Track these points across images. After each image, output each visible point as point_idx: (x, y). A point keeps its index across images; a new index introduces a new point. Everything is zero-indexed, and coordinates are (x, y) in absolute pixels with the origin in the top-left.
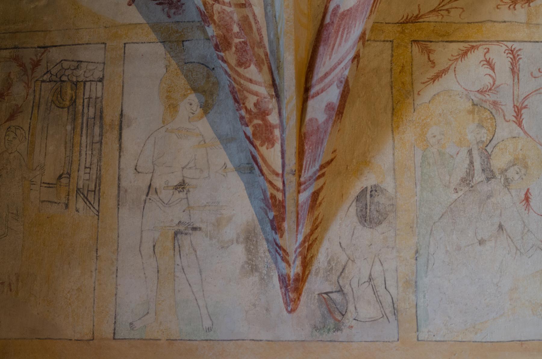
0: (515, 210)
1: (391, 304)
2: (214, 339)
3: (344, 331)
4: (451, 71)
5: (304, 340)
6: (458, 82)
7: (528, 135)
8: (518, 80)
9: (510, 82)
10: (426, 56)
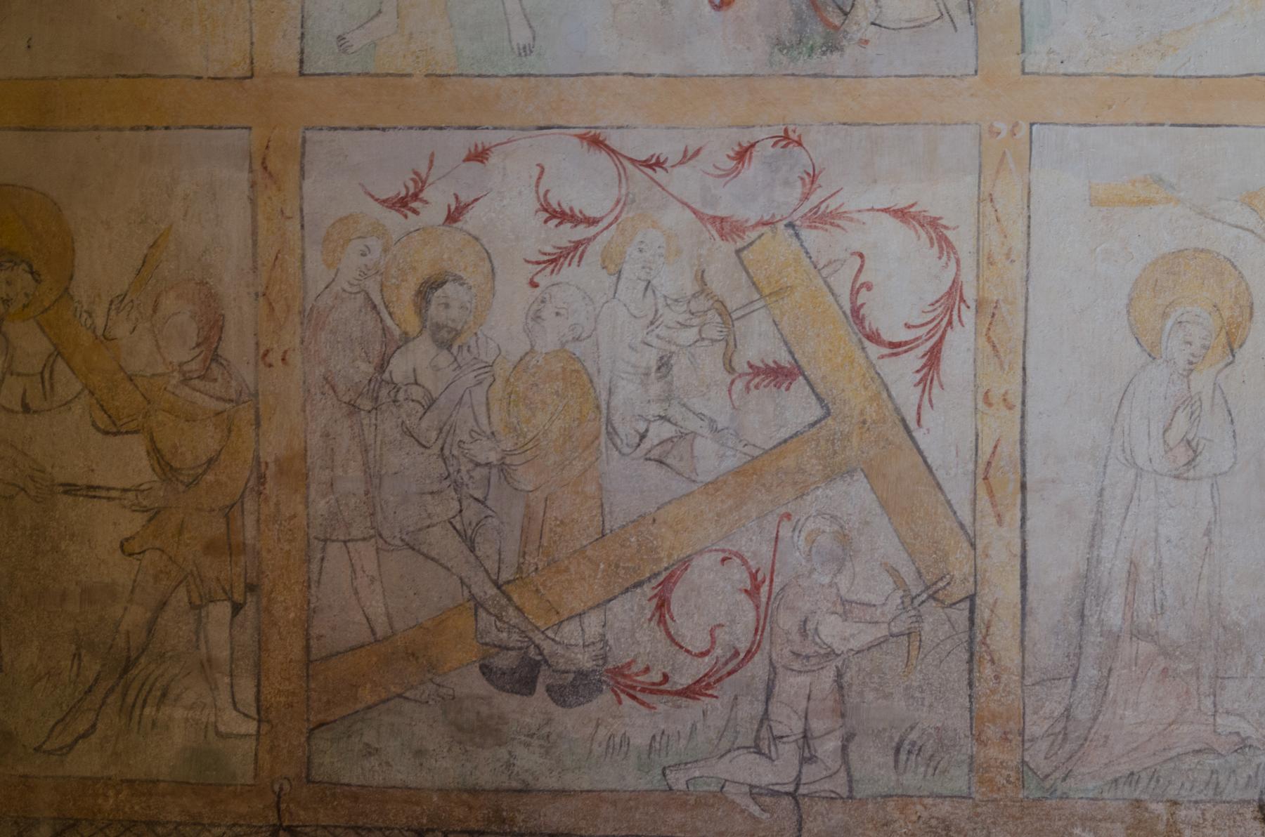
2: (537, 73)
3: (848, 51)
5: (751, 73)
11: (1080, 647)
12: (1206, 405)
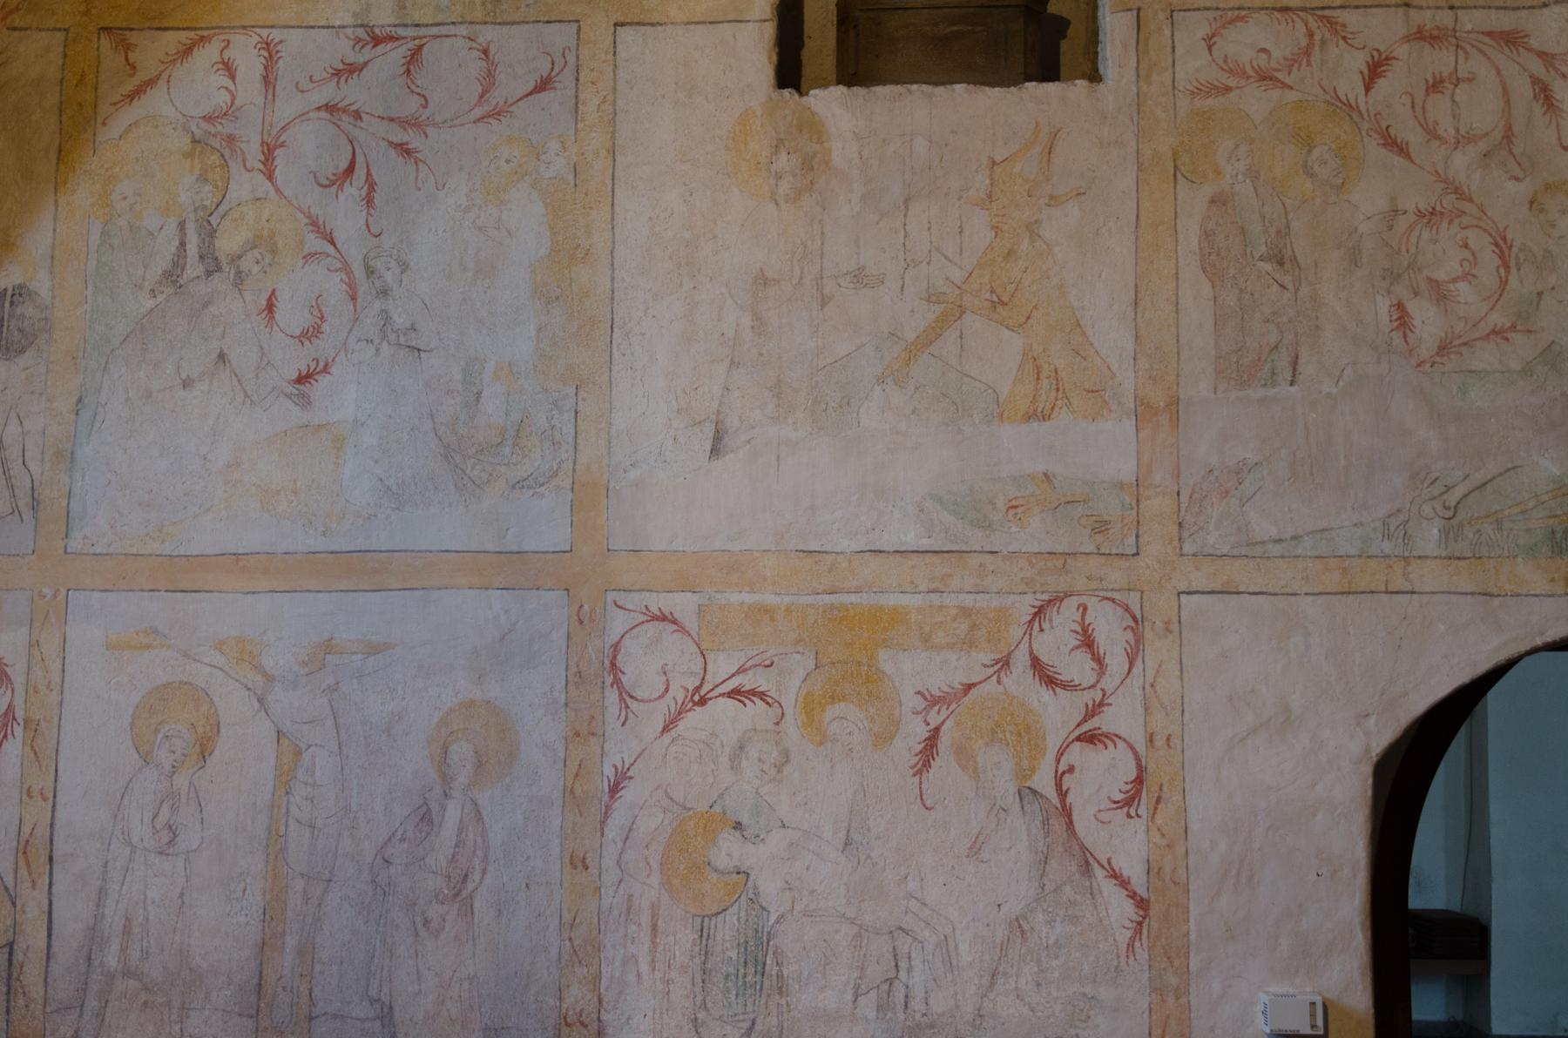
0: (249, 326)
1: (30, 492)
4: (162, 83)
6: (171, 101)
7: (282, 194)
8: (274, 96)
9: (260, 100)
10: (123, 54)
11: (86, 984)
12: (183, 800)
